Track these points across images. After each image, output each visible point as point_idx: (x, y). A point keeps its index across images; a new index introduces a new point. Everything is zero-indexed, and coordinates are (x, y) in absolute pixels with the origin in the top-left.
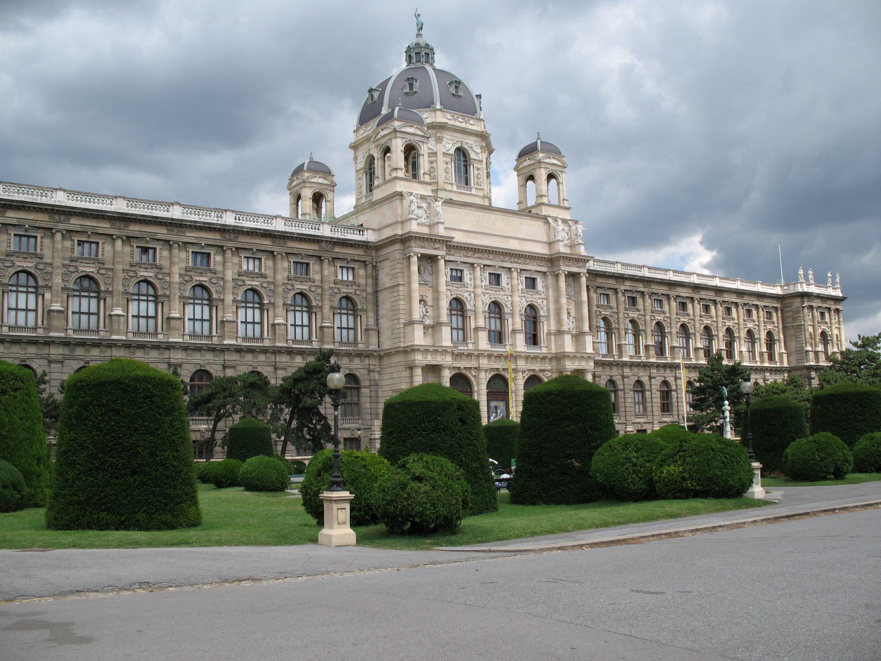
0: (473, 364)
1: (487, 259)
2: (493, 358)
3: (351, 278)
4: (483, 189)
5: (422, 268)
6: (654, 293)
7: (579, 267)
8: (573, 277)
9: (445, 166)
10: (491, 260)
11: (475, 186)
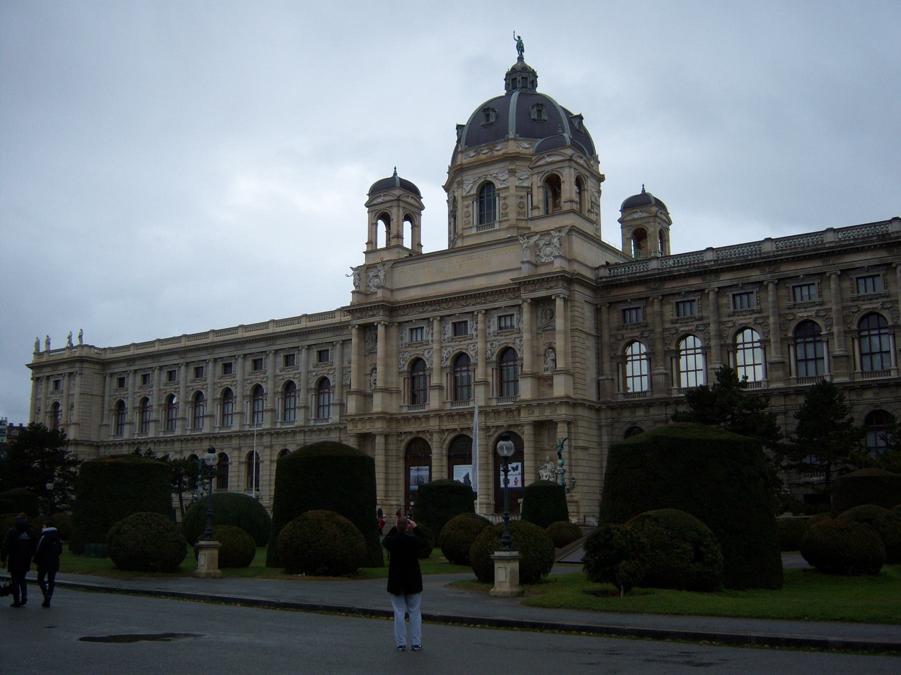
2: (445, 418)
4: (509, 220)
6: (790, 278)
7: (547, 289)
8: (543, 305)
10: (449, 308)
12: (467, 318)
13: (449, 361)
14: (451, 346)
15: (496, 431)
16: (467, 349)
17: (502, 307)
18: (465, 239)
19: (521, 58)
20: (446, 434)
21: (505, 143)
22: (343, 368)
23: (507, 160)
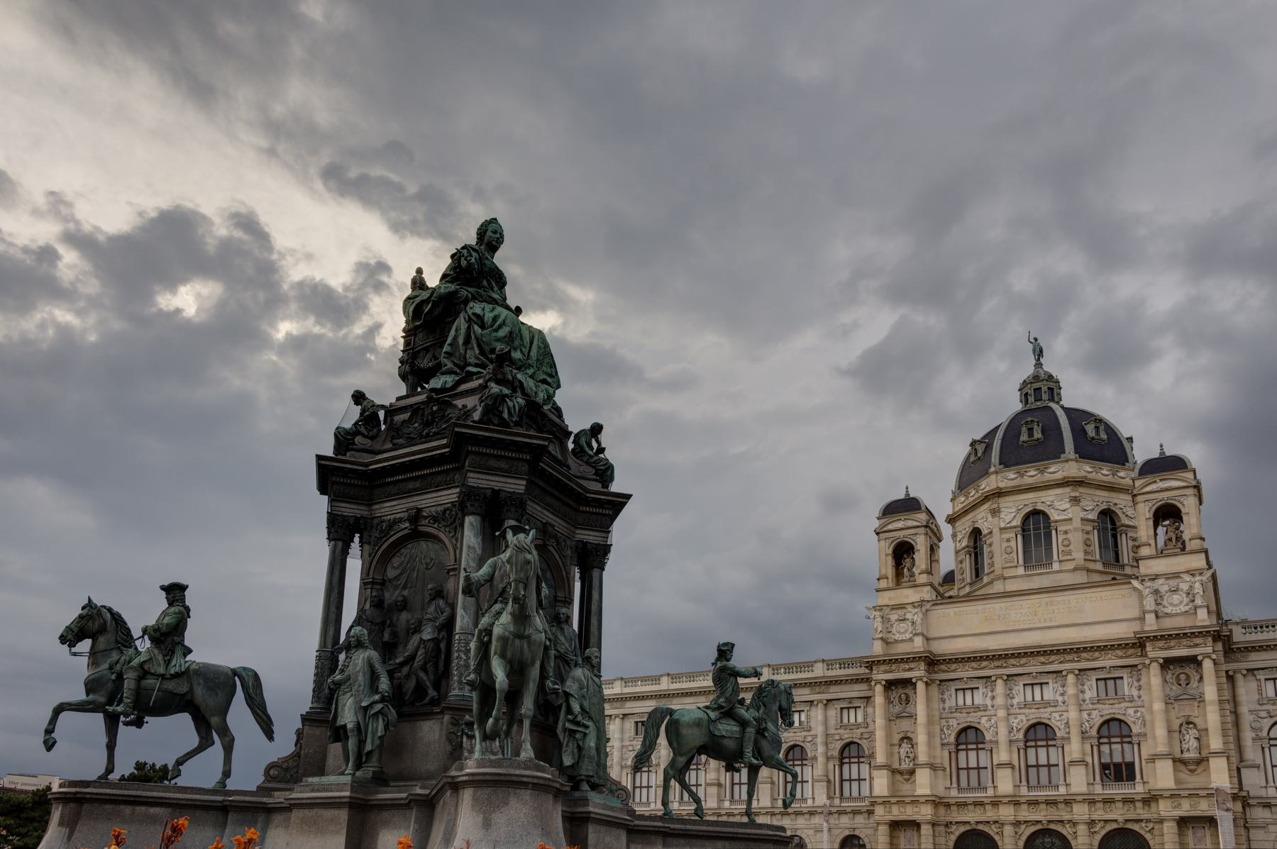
0: (990, 814)
1: (1014, 666)
2: (1025, 807)
3: (860, 719)
4: (1074, 559)
5: (903, 695)
9: (1005, 544)
10: (1021, 666)
11: (1061, 558)
12: (1048, 679)
13: (1022, 733)
14: (1024, 714)
15: (1104, 827)
16: (1049, 719)
17: (1105, 667)
18: (1006, 581)
19: (1039, 365)
20: (1023, 827)
21: (1062, 465)
22: (827, 735)
23: (1068, 486)
